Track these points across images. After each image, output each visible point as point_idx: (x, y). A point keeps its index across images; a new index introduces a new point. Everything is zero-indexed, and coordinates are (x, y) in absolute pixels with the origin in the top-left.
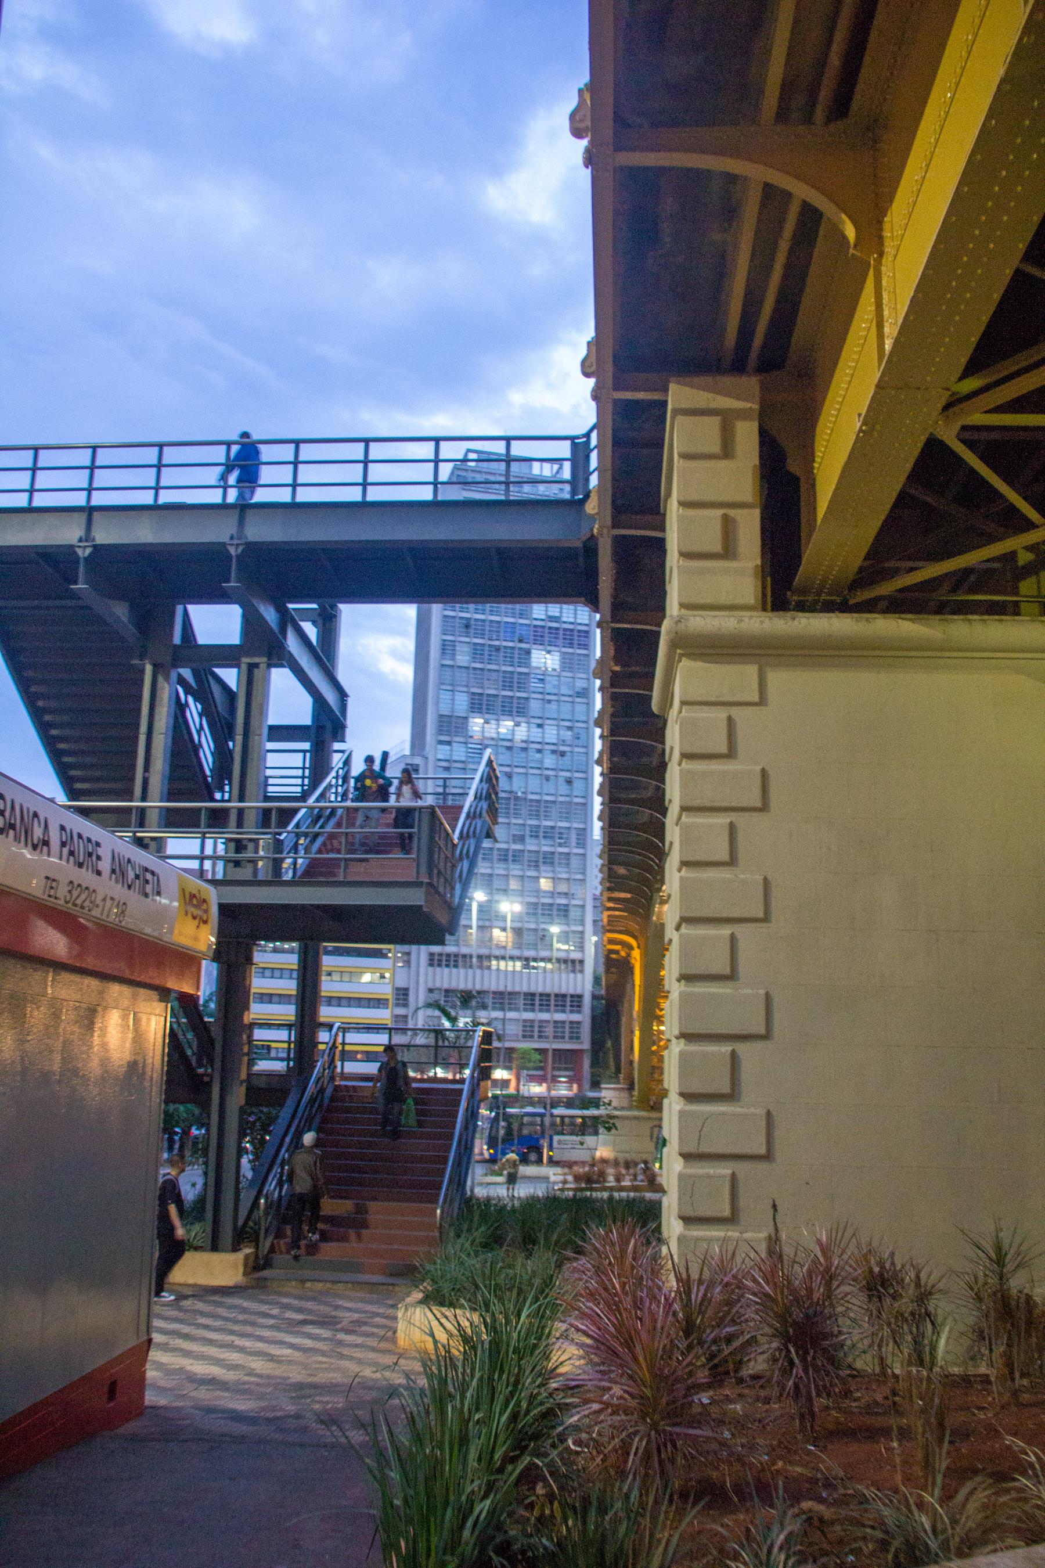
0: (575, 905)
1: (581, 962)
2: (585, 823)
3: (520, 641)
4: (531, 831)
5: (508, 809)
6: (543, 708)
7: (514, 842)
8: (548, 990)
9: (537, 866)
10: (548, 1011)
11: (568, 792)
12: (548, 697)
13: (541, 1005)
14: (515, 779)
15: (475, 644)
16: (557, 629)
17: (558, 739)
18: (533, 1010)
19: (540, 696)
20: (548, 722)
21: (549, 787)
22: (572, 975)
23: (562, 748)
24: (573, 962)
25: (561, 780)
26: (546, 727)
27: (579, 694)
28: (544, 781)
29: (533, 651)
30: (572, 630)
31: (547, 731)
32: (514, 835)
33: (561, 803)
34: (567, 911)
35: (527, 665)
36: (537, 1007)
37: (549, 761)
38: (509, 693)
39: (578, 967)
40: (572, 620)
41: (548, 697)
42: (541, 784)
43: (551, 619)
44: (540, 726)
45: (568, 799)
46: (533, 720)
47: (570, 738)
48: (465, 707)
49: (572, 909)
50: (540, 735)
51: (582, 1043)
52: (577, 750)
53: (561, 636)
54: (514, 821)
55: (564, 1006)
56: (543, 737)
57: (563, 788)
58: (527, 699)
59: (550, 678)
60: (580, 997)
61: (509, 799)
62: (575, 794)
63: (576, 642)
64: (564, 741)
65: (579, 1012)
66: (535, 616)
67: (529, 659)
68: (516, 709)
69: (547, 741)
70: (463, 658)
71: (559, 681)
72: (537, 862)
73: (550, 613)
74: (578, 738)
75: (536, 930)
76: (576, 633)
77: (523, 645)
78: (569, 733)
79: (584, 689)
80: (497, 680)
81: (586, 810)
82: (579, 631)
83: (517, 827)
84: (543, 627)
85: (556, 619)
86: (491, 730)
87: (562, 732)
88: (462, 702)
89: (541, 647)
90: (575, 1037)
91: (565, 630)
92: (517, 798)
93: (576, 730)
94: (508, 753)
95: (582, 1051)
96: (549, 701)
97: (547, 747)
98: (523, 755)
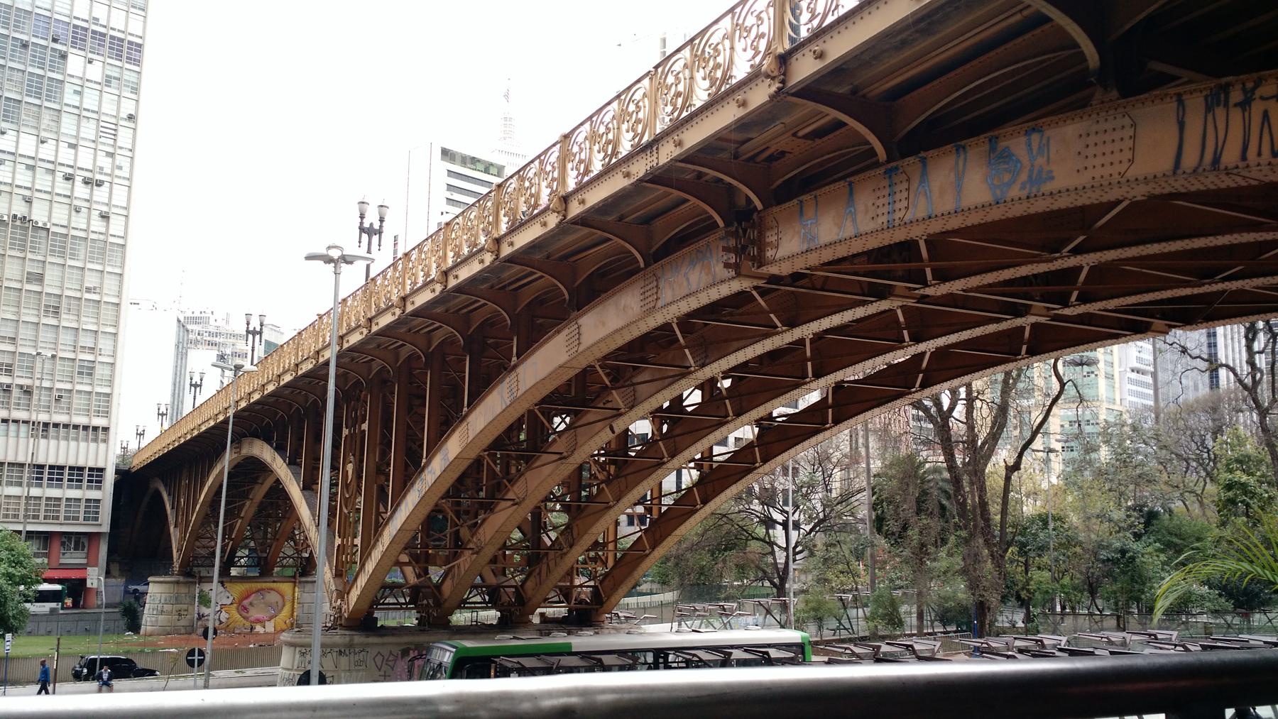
2: (122, 266)
3: (55, 40)
5: (25, 241)
7: (29, 281)
10: (60, 486)
11: (103, 230)
12: (85, 113)
13: (69, 480)
14: (35, 204)
16: (104, 35)
18: (40, 485)
21: (79, 221)
22: (93, 445)
23: (98, 177)
24: (95, 429)
25: (95, 214)
26: (80, 148)
28: (74, 213)
30: (122, 40)
31: (79, 153)
32: (28, 273)
34: (93, 368)
37: (81, 191)
38: (37, 102)
41: (85, 113)
45: (102, 237)
49: (98, 366)
50: (73, 157)
52: (116, 180)
53: (108, 45)
54: (30, 256)
55: (81, 481)
57: (97, 225)
59: (90, 91)
60: (102, 470)
62: (111, 232)
63: (125, 55)
64: (101, 168)
65: (99, 488)
67: (65, 64)
73: (94, 15)
74: (120, 168)
75: (50, 389)
76: (126, 45)
78: (110, 160)
80: (22, 83)
81: (124, 253)
82: (130, 43)
83: (36, 264)
84: (86, 30)
87: (99, 158)
89: (82, 53)
91: (112, 37)
92: (36, 228)
94: (30, 173)
95: (98, 534)
98: (50, 178)
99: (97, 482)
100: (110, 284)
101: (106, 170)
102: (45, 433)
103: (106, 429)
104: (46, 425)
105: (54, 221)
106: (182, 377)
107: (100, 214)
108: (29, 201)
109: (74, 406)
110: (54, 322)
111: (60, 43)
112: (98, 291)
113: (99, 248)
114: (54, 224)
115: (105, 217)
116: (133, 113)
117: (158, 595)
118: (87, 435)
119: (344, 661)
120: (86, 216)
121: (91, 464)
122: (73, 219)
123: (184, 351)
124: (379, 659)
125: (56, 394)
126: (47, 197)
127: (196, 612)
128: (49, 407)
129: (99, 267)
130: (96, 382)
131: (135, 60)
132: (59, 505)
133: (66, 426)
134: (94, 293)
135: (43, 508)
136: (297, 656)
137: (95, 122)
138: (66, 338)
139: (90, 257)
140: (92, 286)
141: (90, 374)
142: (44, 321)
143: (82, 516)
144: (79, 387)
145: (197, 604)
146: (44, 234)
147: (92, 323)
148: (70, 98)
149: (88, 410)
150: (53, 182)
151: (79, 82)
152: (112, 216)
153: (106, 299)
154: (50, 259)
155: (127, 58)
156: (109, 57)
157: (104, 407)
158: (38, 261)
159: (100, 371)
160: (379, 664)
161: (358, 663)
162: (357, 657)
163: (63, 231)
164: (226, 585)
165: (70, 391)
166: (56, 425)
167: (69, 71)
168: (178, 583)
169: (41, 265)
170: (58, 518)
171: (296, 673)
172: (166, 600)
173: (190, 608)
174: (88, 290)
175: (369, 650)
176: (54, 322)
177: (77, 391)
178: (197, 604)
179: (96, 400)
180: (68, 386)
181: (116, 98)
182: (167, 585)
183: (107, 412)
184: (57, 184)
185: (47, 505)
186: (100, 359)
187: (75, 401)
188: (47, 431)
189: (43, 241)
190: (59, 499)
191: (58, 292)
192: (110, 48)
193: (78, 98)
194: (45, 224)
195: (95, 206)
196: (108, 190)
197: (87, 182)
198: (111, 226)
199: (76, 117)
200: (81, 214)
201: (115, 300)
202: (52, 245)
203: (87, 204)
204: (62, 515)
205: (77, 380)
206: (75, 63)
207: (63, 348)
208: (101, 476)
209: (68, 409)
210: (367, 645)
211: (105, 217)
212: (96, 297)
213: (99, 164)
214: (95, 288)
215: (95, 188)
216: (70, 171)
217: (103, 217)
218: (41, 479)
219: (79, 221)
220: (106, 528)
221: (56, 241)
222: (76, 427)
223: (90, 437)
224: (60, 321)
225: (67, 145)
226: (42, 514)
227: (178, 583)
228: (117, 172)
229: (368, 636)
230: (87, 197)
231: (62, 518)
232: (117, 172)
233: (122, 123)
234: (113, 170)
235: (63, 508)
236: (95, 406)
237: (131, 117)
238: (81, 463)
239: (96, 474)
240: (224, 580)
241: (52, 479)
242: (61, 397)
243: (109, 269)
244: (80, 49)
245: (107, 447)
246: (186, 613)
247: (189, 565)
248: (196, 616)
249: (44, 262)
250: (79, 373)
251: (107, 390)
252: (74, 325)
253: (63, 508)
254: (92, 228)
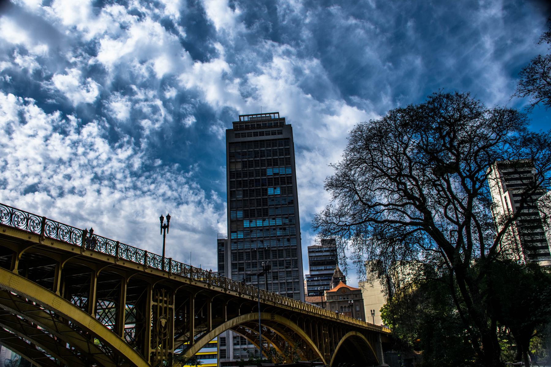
4: (274, 264)
15: (244, 190)
17: (282, 223)
27: (289, 203)
37: (279, 233)
40: (285, 173)
43: (275, 174)
44: (274, 219)
48: (242, 216)
56: (276, 223)
61: (263, 251)
64: (285, 223)
66: (268, 174)
68: (264, 214)
70: (240, 197)
73: (274, 172)
77: (264, 187)
78: (288, 220)
79: (292, 200)
85: (278, 174)
86: (253, 225)
88: (240, 214)
92: (266, 250)
108: (262, 241)
206: (271, 191)
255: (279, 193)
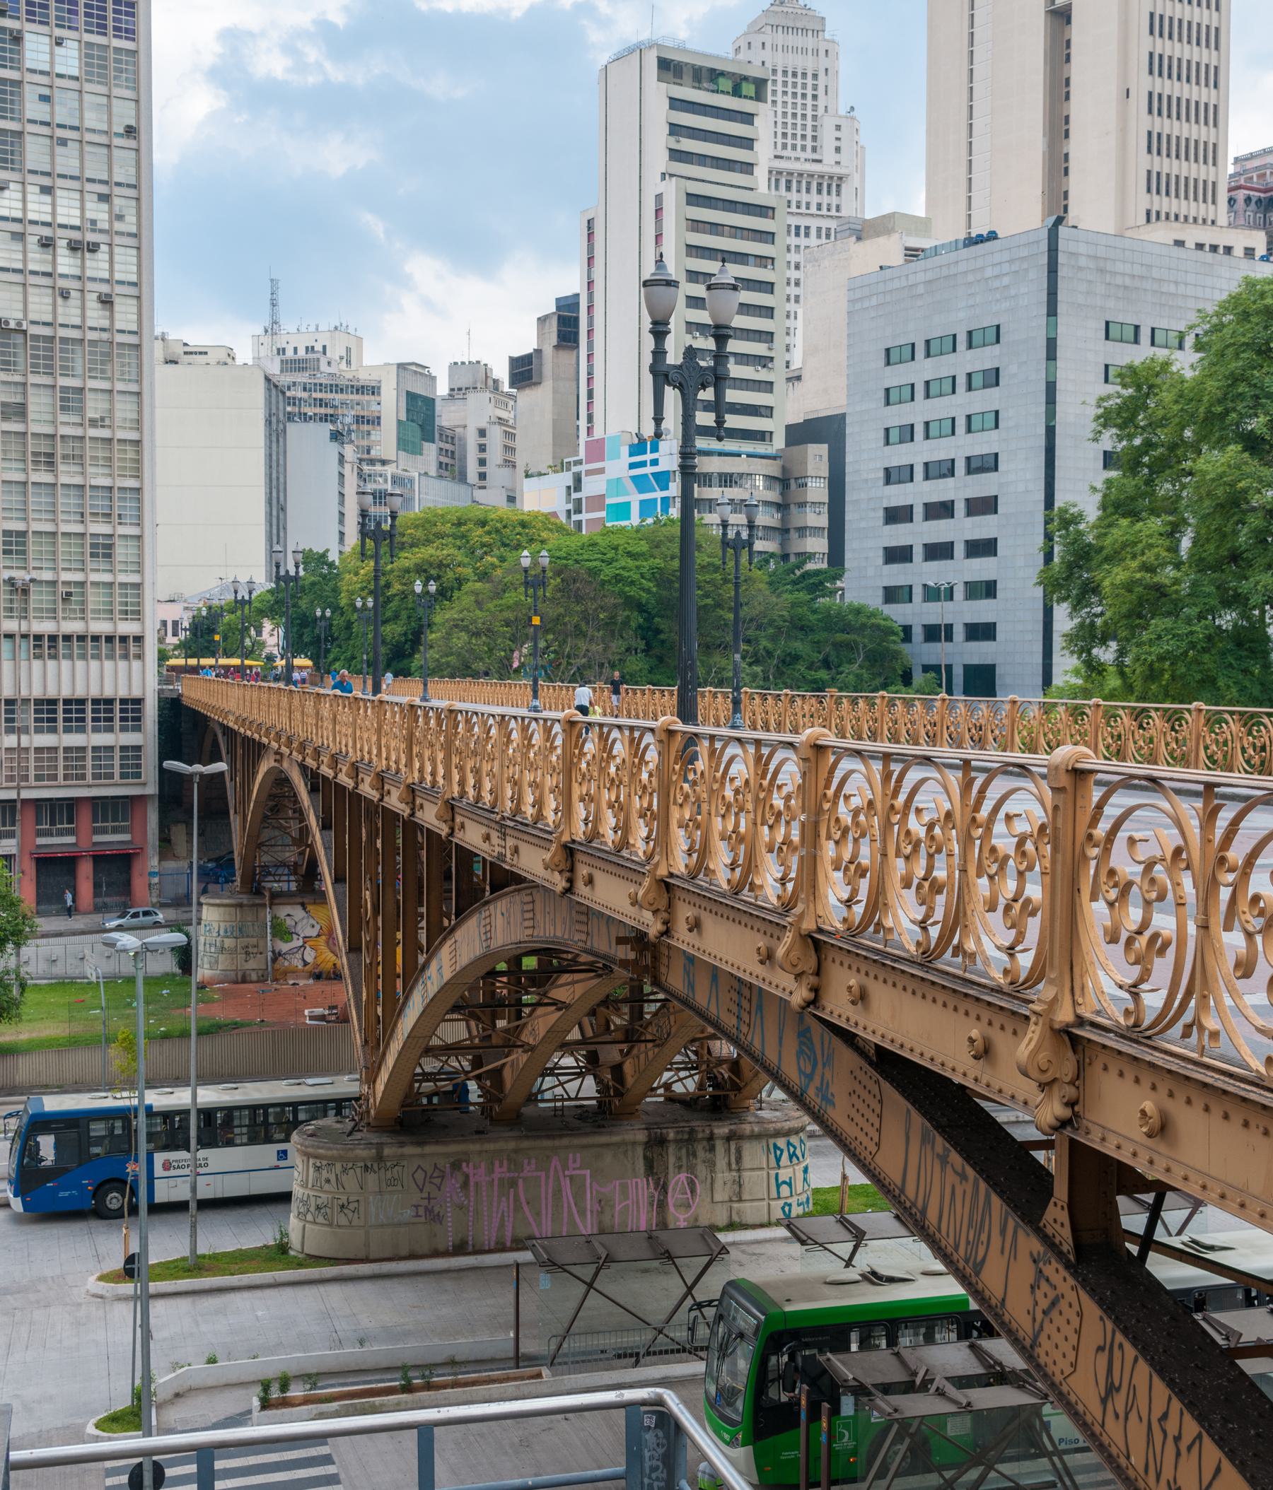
0: (125, 537)
1: (139, 639)
6: (52, 155)
8: (80, 693)
9: (51, 464)
10: (82, 730)
11: (105, 323)
12: (60, 133)
17: (82, 217)
18: (54, 730)
19: (45, 130)
20: (60, 182)
21: (68, 311)
22: (122, 664)
23: (91, 237)
24: (124, 639)
26: (59, 193)
28: (60, 301)
29: (27, 36)
31: (59, 201)
33: (93, 343)
34: (110, 546)
35: (17, 64)
36: (60, 724)
37: (66, 263)
39: (133, 649)
41: (60, 133)
42: (54, 305)
44: (47, 190)
45: (105, 336)
46: (31, 178)
47: (106, 216)
49: (118, 542)
50: (48, 209)
51: (144, 784)
55: (111, 720)
56: (54, 214)
57: (96, 315)
58: (20, 134)
60: (139, 701)
62: (118, 326)
63: (110, 24)
64: (94, 222)
65: (137, 729)
69: (60, 220)
71: (81, 101)
72: (51, 455)
74: (120, 218)
78: (105, 207)
83: (13, 389)
87: (88, 205)
90: (132, 771)
93: (116, 201)
96: (63, 142)
97: (60, 232)
98: (19, 247)
99: (134, 719)
100: (124, 409)
101: (100, 225)
102: (52, 651)
103: (139, 639)
104: (53, 638)
105: (32, 317)
106: (281, 469)
107: (99, 297)
109: (90, 606)
110: (47, 478)
111: (11, 17)
112: (107, 422)
113: (102, 354)
114: (33, 322)
115: (106, 301)
116: (133, 123)
117: (215, 925)
118: (113, 650)
119: (371, 1178)
120: (79, 303)
121: (123, 693)
122: (60, 310)
123: (281, 426)
124: (420, 1176)
125: (62, 589)
126: (17, 278)
127: (270, 948)
128: (54, 611)
129: (105, 385)
130: (118, 568)
131: (127, 31)
132: (84, 759)
133: (82, 638)
134: (103, 426)
135: (61, 763)
136: (311, 1170)
137: (77, 145)
138: (66, 501)
139: (90, 370)
140: (98, 416)
141: (109, 556)
142: (35, 477)
143: (117, 771)
144: (94, 577)
145: (269, 937)
146: (19, 339)
147: (103, 475)
148: (34, 109)
149: (111, 612)
150: (25, 252)
151: (44, 80)
152: (117, 300)
153: (121, 434)
154: (33, 379)
155: (116, 29)
156: (86, 31)
157: (132, 604)
158: (16, 384)
159: (122, 552)
160: (420, 1183)
161: (391, 1182)
162: (389, 1175)
163: (47, 331)
164: (309, 907)
165: (82, 584)
166: (67, 638)
167: (29, 64)
168: (240, 906)
169: (20, 389)
170: (83, 777)
171: (311, 1193)
172: (226, 931)
173: (261, 943)
174: (94, 423)
175: (405, 1163)
176: (47, 478)
177: (93, 583)
178: (269, 937)
179: (121, 595)
180: (78, 577)
181: (104, 100)
182: (222, 909)
183: (138, 612)
184: (30, 255)
185: (66, 759)
186: (121, 530)
187: (90, 598)
188: (55, 647)
189: (20, 351)
190: (83, 749)
191: (48, 430)
192: (87, 15)
193: (45, 107)
194: (19, 324)
195: (90, 286)
196: (106, 257)
197: (74, 247)
198: (117, 316)
199: (48, 141)
200: (72, 302)
201: (133, 436)
202: (33, 356)
203: (75, 284)
204: (89, 772)
205: (90, 566)
207: (65, 517)
208: (139, 711)
209: (83, 611)
210: (402, 1156)
211: (106, 301)
212: (105, 433)
213: (89, 215)
214: (102, 419)
215: (87, 255)
216: (46, 232)
217: (103, 302)
218: (55, 720)
219: (68, 311)
220: (152, 789)
221: (37, 348)
222: (96, 638)
223: (118, 652)
224: (56, 476)
225: (37, 189)
226: (61, 772)
227: (240, 906)
228: (118, 226)
229: (402, 1144)
230: (77, 272)
231: (89, 776)
232: (118, 226)
233: (117, 141)
234: (111, 222)
235: (89, 763)
236: (121, 603)
237: (131, 131)
238: (108, 693)
239: (133, 706)
240: (306, 901)
241: (69, 720)
242: (69, 594)
243: (120, 386)
244: (41, 22)
245: (144, 666)
246: (255, 950)
247: (253, 880)
248: (270, 954)
249: (24, 384)
250: (92, 555)
251: (134, 578)
252: (78, 480)
253: (89, 763)
254: (90, 323)
255: (75, 72)
